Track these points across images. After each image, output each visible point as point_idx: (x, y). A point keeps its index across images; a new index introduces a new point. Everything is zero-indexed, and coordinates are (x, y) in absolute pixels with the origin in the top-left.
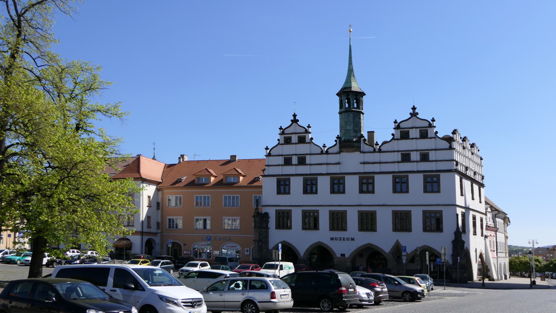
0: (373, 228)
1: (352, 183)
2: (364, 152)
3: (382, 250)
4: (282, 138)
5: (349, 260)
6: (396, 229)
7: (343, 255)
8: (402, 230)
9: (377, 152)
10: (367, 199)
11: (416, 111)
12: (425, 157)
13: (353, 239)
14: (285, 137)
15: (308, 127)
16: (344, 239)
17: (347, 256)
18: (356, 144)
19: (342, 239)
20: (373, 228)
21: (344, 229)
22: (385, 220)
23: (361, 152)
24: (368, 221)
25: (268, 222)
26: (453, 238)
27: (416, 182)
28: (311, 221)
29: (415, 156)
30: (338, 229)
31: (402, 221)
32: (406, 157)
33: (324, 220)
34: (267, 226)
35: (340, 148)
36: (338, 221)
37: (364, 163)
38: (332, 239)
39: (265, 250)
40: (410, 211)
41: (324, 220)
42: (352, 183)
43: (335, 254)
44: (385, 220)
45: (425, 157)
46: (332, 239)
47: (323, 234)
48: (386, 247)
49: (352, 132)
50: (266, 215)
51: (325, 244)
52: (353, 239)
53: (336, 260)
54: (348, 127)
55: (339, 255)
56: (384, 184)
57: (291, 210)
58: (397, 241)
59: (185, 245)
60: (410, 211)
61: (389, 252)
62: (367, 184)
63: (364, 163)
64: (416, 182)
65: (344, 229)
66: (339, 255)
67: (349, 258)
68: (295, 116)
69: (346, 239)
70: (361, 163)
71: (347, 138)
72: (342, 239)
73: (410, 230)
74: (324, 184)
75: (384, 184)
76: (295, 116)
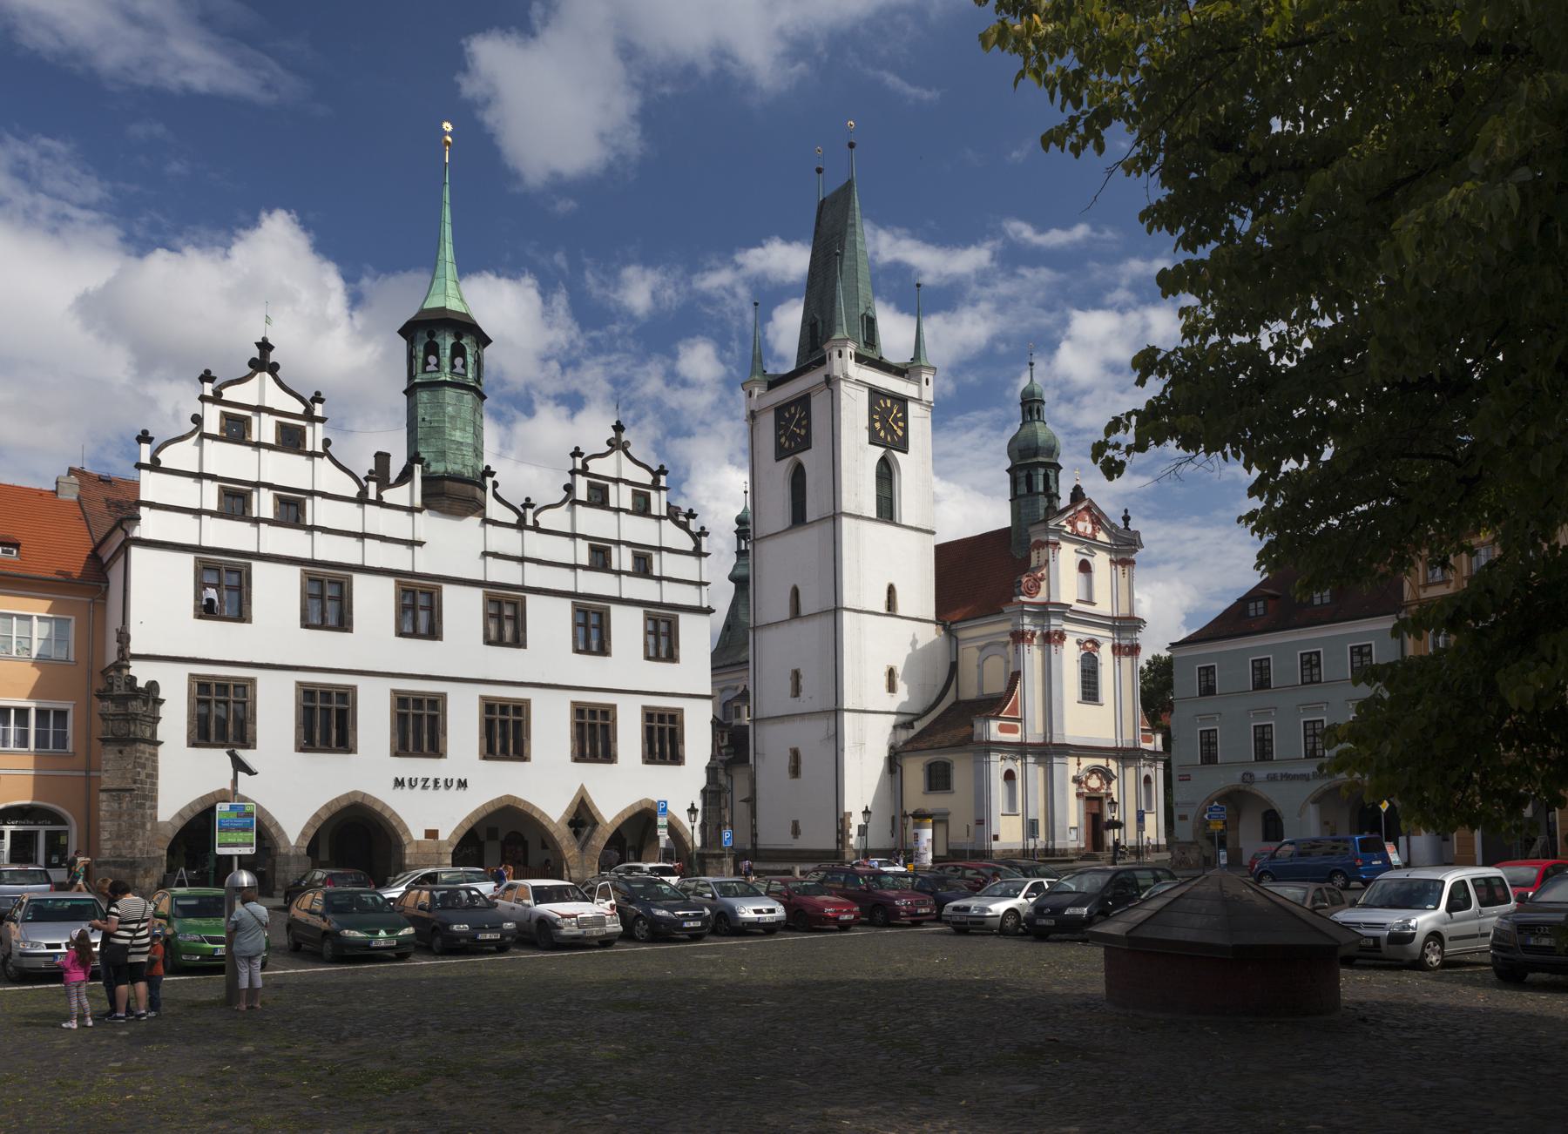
0: (519, 752)
1: (463, 611)
2: (495, 523)
3: (543, 814)
5: (451, 850)
6: (580, 756)
7: (432, 834)
8: (594, 758)
10: (504, 663)
11: (624, 437)
12: (643, 567)
13: (463, 784)
16: (436, 781)
17: (444, 836)
19: (430, 783)
20: (519, 752)
21: (435, 749)
22: (551, 727)
24: (506, 732)
27: (627, 627)
28: (326, 721)
29: (623, 559)
30: (418, 752)
31: (593, 735)
32: (600, 557)
33: (374, 718)
36: (419, 726)
37: (496, 555)
38: (399, 783)
40: (614, 707)
41: (374, 718)
42: (463, 611)
43: (406, 830)
44: (551, 727)
45: (643, 567)
46: (399, 783)
47: (370, 769)
48: (554, 808)
51: (376, 800)
52: (463, 784)
53: (408, 851)
55: (418, 835)
56: (549, 622)
57: (253, 681)
58: (582, 789)
60: (614, 707)
61: (562, 820)
63: (496, 555)
64: (627, 627)
65: (435, 749)
66: (418, 835)
67: (449, 842)
69: (441, 783)
70: (485, 554)
71: (457, 468)
72: (430, 783)
73: (608, 756)
74: (374, 601)
75: (549, 622)
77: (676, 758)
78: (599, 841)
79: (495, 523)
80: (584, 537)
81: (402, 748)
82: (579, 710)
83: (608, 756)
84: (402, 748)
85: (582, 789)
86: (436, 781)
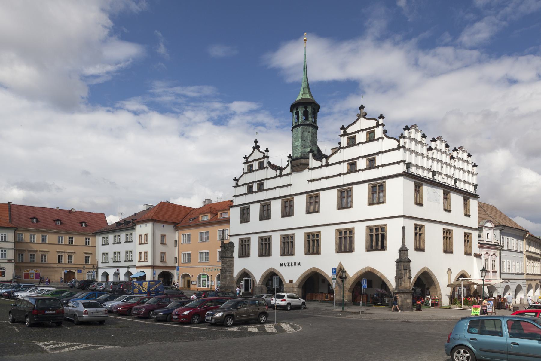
2: (312, 169)
3: (326, 274)
4: (246, 167)
9: (324, 166)
14: (248, 166)
15: (265, 151)
16: (291, 264)
18: (303, 161)
19: (290, 264)
21: (292, 254)
22: (329, 240)
23: (310, 169)
24: (313, 244)
25: (233, 251)
26: (397, 257)
27: (361, 194)
34: (232, 255)
35: (292, 168)
38: (282, 265)
39: (228, 278)
42: (300, 203)
44: (329, 240)
47: (275, 261)
49: (299, 148)
50: (231, 244)
52: (299, 264)
54: (297, 144)
56: (328, 200)
58: (340, 264)
59: (192, 276)
62: (313, 202)
64: (361, 194)
68: (256, 142)
70: (309, 181)
72: (290, 264)
73: (351, 250)
75: (328, 200)
76: (256, 142)
77: (383, 248)
78: (348, 285)
79: (312, 169)
80: (344, 162)
81: (283, 254)
82: (340, 232)
83: (351, 250)
84: (283, 254)
85: (340, 264)
86: (291, 264)
